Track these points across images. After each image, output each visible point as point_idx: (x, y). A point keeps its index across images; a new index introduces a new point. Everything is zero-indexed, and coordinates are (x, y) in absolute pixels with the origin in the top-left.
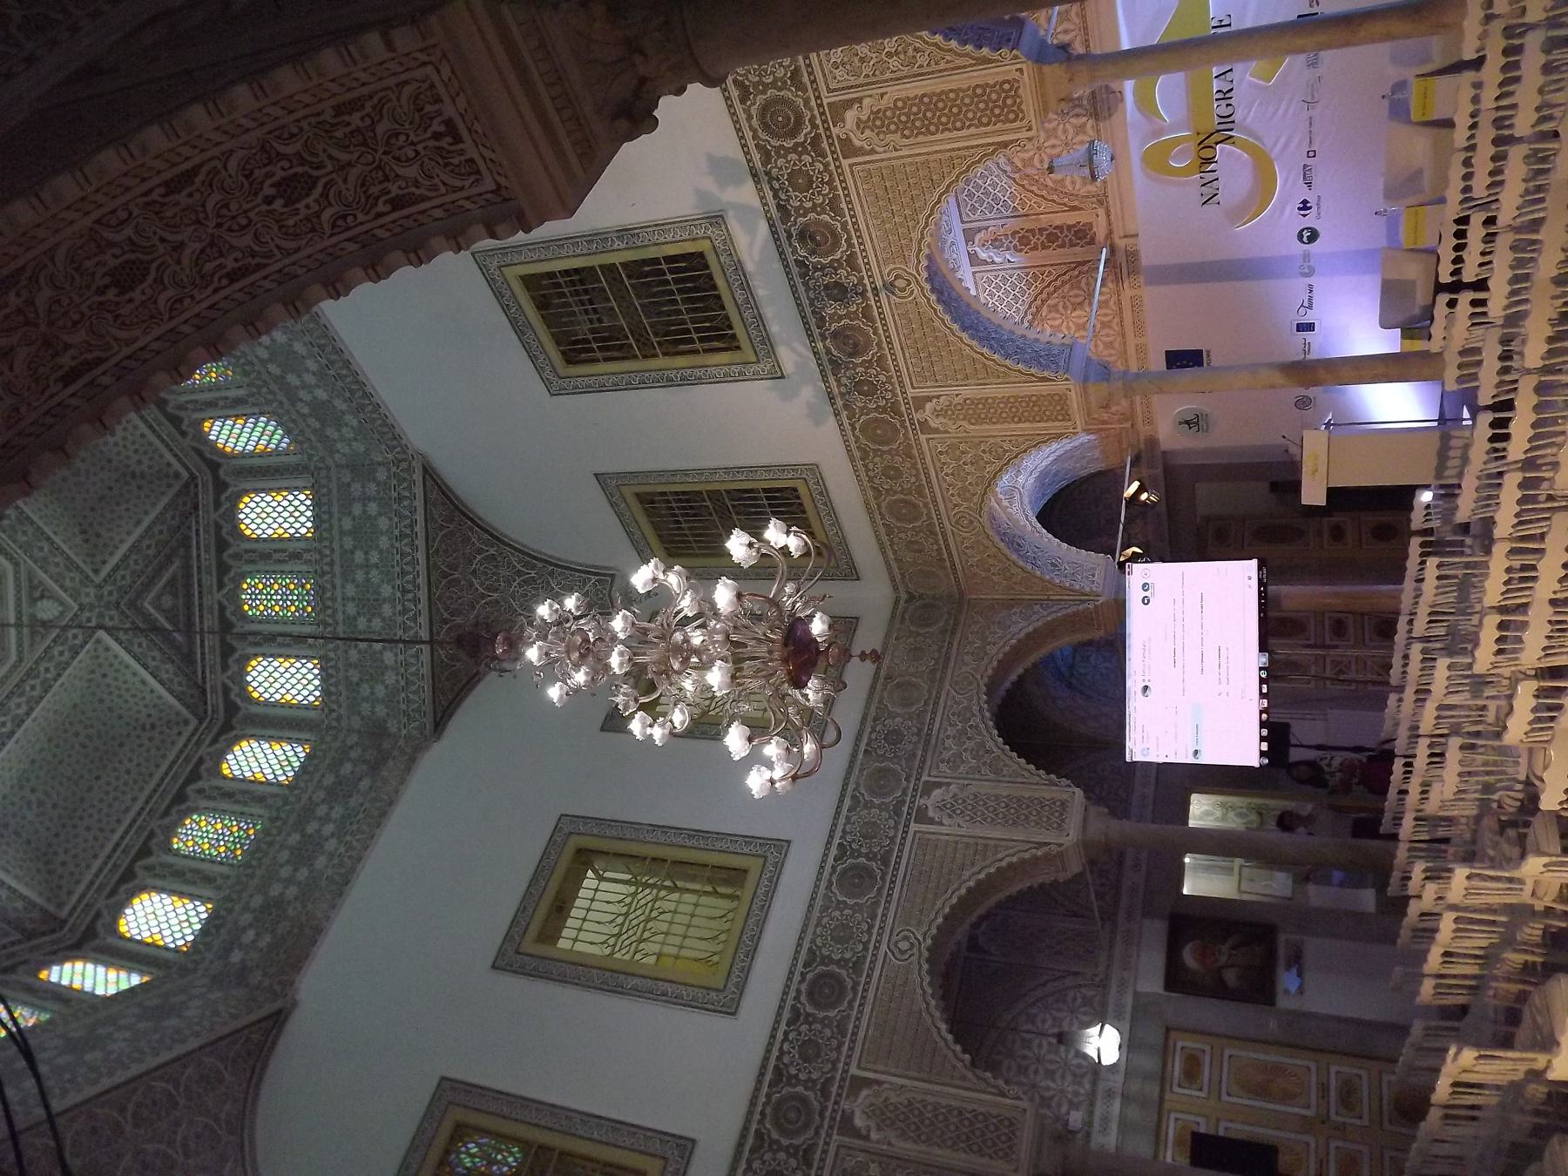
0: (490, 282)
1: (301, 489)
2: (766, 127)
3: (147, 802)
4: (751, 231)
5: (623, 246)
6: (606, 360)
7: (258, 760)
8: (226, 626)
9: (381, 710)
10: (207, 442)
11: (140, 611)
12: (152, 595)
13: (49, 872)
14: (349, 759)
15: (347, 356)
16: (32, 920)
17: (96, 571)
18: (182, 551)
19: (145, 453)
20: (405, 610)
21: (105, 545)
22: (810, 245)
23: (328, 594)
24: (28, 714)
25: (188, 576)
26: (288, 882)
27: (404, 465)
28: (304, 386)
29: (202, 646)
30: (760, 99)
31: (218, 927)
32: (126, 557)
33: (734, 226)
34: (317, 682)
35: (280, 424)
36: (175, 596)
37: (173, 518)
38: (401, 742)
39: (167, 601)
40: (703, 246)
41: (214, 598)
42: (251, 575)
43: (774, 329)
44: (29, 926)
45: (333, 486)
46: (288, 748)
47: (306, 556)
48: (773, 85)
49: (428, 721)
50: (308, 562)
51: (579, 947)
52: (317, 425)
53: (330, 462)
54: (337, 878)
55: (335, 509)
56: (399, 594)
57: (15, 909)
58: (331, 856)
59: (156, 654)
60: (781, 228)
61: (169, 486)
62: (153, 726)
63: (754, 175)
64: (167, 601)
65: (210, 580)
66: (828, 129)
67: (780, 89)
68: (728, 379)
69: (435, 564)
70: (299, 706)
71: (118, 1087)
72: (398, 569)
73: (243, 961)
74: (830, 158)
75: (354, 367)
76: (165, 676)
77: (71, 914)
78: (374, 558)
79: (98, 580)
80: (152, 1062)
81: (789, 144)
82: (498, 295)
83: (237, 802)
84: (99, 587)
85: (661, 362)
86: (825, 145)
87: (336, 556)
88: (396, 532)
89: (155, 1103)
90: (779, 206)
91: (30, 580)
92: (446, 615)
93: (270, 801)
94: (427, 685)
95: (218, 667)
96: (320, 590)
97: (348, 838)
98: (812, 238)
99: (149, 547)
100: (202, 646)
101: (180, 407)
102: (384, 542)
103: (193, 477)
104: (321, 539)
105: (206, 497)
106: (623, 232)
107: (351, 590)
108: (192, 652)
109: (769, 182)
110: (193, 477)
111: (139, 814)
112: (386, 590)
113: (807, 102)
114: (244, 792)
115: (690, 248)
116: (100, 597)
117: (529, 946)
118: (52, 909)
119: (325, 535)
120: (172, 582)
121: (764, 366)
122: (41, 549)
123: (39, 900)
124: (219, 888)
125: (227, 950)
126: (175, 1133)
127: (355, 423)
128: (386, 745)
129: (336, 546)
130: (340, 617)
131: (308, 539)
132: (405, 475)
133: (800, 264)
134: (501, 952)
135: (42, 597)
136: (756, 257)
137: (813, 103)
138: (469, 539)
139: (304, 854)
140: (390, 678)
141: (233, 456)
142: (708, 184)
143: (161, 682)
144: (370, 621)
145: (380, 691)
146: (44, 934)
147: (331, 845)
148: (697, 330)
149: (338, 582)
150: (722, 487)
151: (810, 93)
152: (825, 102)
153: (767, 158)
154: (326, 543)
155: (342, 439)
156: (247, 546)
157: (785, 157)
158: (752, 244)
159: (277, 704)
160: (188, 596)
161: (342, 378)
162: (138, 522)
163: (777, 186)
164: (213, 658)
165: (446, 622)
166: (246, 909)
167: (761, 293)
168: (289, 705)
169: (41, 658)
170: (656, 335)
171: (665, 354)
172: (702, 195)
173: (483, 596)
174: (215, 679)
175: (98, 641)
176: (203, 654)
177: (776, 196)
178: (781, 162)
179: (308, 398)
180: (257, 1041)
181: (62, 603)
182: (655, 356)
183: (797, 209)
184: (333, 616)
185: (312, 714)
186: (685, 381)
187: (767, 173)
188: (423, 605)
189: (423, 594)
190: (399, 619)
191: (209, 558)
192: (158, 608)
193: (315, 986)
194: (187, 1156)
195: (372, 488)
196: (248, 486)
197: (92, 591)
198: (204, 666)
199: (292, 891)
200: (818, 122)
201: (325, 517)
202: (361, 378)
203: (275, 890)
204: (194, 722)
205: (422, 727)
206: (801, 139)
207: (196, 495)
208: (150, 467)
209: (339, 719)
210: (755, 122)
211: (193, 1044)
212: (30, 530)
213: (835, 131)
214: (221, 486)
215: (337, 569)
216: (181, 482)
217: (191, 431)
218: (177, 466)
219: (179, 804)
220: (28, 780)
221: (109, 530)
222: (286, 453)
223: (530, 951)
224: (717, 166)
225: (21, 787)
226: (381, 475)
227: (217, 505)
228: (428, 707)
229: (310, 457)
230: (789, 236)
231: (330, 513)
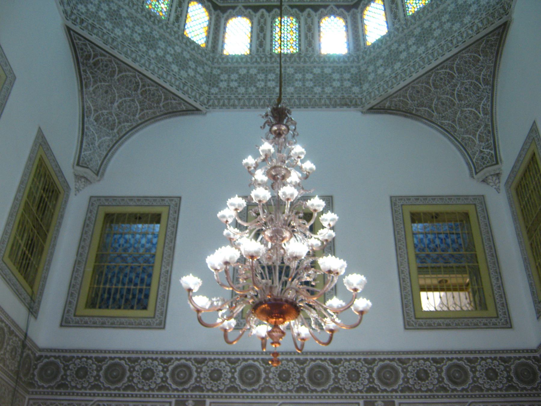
80: (434, 64)
211: (455, 51)
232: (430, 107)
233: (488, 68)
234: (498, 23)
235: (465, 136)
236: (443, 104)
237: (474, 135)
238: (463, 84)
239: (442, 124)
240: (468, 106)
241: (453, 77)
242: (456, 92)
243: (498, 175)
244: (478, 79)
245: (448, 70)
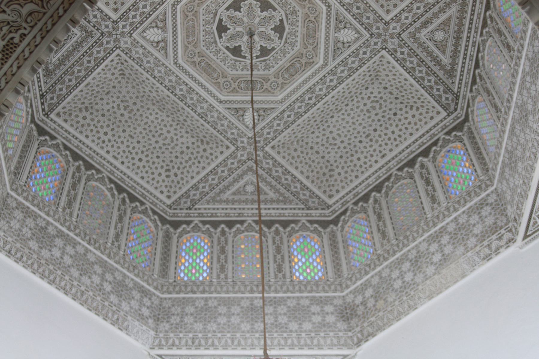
19: (83, 126)
91: (166, 53)
110: (47, 115)
135: (158, 42)
207: (42, 104)
212: (167, 83)
216: (56, 111)
218: (60, 121)
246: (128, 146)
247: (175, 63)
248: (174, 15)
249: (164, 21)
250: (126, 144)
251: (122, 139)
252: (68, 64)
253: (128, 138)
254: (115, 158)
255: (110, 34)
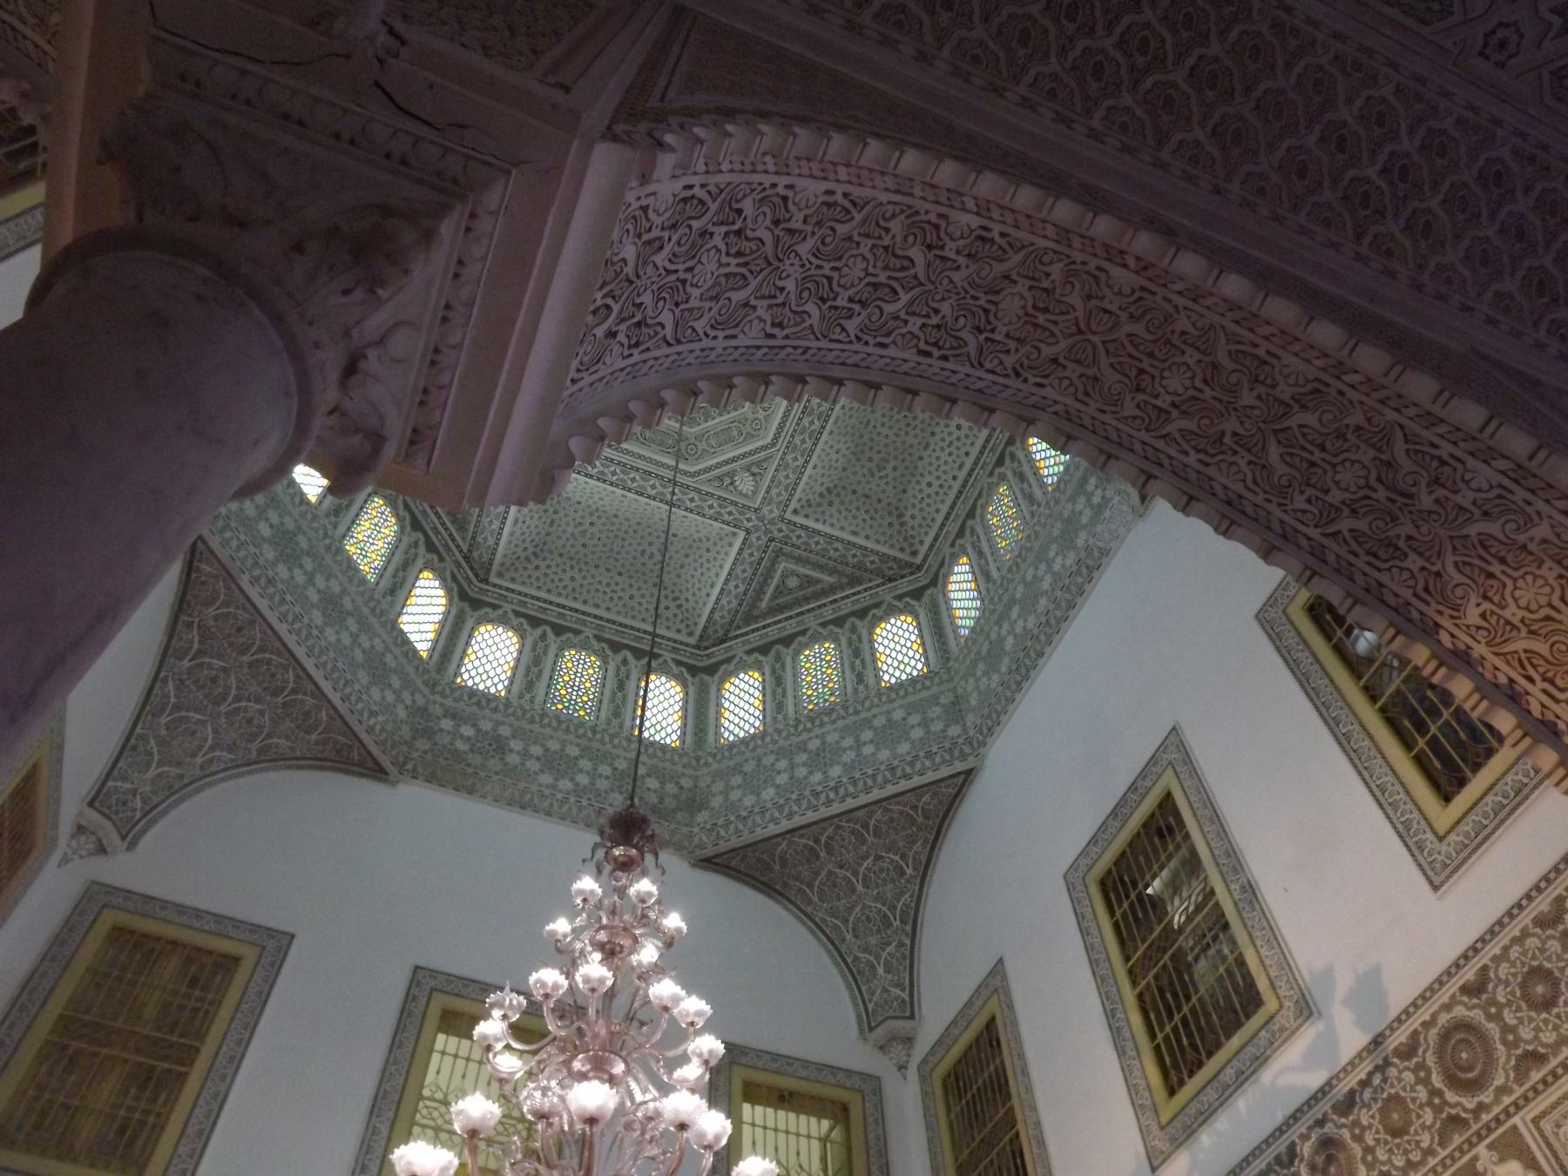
0: (1153, 760)
1: (927, 663)
2: (1445, 1037)
3: (608, 621)
4: (1310, 1060)
5: (1236, 897)
6: (1116, 926)
7: (663, 708)
8: (787, 641)
9: (716, 802)
10: (951, 567)
11: (774, 562)
12: (794, 567)
13: (527, 558)
14: (663, 783)
15: (1048, 650)
16: (481, 556)
17: (795, 512)
18: (846, 580)
20: (817, 794)
21: (823, 513)
22: (1320, 1160)
23: (826, 719)
24: (649, 497)
25: (823, 593)
26: (525, 754)
27: (967, 750)
28: (1013, 624)
29: (764, 627)
30: (1477, 1015)
31: (478, 704)
32: (817, 532)
33: (1308, 1035)
34: (742, 734)
35: (978, 620)
36: (801, 587)
37: (872, 562)
38: (685, 830)
39: (793, 582)
40: (1271, 1004)
41: (811, 622)
42: (838, 647)
43: (1205, 1138)
44: (475, 554)
45: (935, 690)
46: (675, 727)
47: (861, 688)
48: (1506, 1029)
49: (710, 851)
50: (856, 691)
51: (436, 1057)
52: (984, 651)
53: (957, 679)
54: (528, 797)
55: (911, 699)
56: (832, 784)
57: (485, 539)
58: (554, 787)
59: (742, 588)
60: (1325, 1106)
61: (902, 549)
62: (680, 606)
63: (1377, 1042)
64: (793, 582)
65: (828, 614)
66: (1481, 1138)
67: (1504, 1042)
68: (1132, 1089)
69: (873, 812)
70: (718, 726)
71: (281, 640)
72: (857, 776)
73: (441, 730)
74: (1443, 1153)
75: (1041, 661)
76: (724, 602)
77: (495, 585)
78: (868, 750)
79: (788, 515)
80: (309, 664)
81: (1437, 1081)
82: (1143, 774)
83: (614, 694)
84: (782, 519)
85: (1129, 995)
86: (1457, 1140)
87: (864, 715)
88: (896, 763)
89: (273, 675)
90: (1352, 1093)
92: (823, 839)
93: (615, 722)
94: (747, 838)
95: (748, 647)
96: (830, 711)
97: (572, 800)
98: (1330, 1159)
99: (836, 550)
100: (764, 627)
101: (973, 531)
102: (885, 754)
103: (919, 568)
104: (879, 694)
105: (904, 586)
106: (1250, 890)
107: (830, 739)
108: (756, 619)
109: (1377, 1068)
110: (919, 568)
111: (595, 617)
112: (835, 771)
113: (1503, 1090)
114: (625, 698)
115: (1262, 984)
116: (772, 522)
117: (439, 1001)
118: (495, 568)
119: (884, 698)
120: (811, 581)
121: (1160, 1143)
122: (795, 459)
123: (499, 556)
124: (521, 696)
125: (453, 715)
126: (249, 700)
127: (993, 685)
128: (680, 816)
129: (875, 711)
130: (805, 736)
131: (878, 684)
132: (956, 753)
133: (1292, 1152)
134: (433, 973)
136: (1284, 1081)
137: (1507, 1100)
138: (914, 842)
139: (556, 763)
140: (749, 801)
141: (945, 593)
142: (1344, 982)
143: (718, 599)
144: (804, 764)
145: (735, 795)
146: (472, 568)
147: (566, 785)
148: (1175, 1029)
149: (840, 724)
150: (1020, 1126)
151: (1519, 1092)
152: (1516, 1120)
153: (1408, 1051)
154: (876, 701)
155: (977, 680)
156: (864, 633)
157: (1419, 1081)
158: (1293, 1070)
159: (719, 705)
160: (807, 599)
161: (1028, 655)
162: (855, 533)
163: (1377, 1080)
164: (755, 639)
165: (817, 841)
166: (563, 743)
167: (1242, 1103)
168: (719, 715)
169: (699, 491)
170: (1156, 977)
171: (1140, 997)
172: (1328, 974)
173: (856, 873)
174: (738, 647)
175: (734, 534)
176: (757, 629)
177: (1364, 1084)
178: (1408, 1077)
179: (1004, 632)
180: (353, 757)
181: (754, 493)
182: (1134, 984)
183: (1356, 1123)
184: (805, 729)
185: (711, 738)
186: (1116, 1033)
187: (1387, 1063)
188: (824, 812)
189: (837, 808)
190: (807, 792)
191: (846, 607)
192: (784, 577)
193: (412, 803)
194: (228, 714)
195: (937, 727)
196: (922, 618)
197: (776, 513)
198: (747, 633)
199: (513, 759)
200: (1485, 1118)
201: (902, 693)
202: (1033, 673)
203: (516, 745)
204: (693, 641)
205: (702, 846)
206: (1451, 1097)
207: (903, 577)
208: (913, 528)
209: (707, 764)
210: (1443, 1019)
211: (335, 698)
213: (1481, 1149)
214: (917, 594)
215: (853, 718)
217: (956, 549)
218: (923, 550)
219: (610, 645)
220: (599, 517)
221: (839, 512)
222: (957, 636)
223: (432, 1004)
224: (1370, 984)
225: (591, 514)
226: (954, 731)
227: (899, 598)
228: (723, 846)
229: (956, 659)
230: (1320, 1123)
231: (907, 694)
232: (200, 653)
233: (292, 749)
234: (385, 761)
235: (152, 742)
236: (214, 680)
237: (161, 763)
238: (262, 713)
239: (165, 681)
240: (216, 731)
241: (275, 694)
242: (243, 704)
243: (102, 850)
244: (269, 736)
245: (291, 685)
246: (942, 449)
247: (774, 445)
248: (706, 471)
249: (720, 478)
250: (938, 453)
251: (933, 459)
252: (832, 563)
253: (929, 452)
254: (961, 467)
255: (767, 531)
